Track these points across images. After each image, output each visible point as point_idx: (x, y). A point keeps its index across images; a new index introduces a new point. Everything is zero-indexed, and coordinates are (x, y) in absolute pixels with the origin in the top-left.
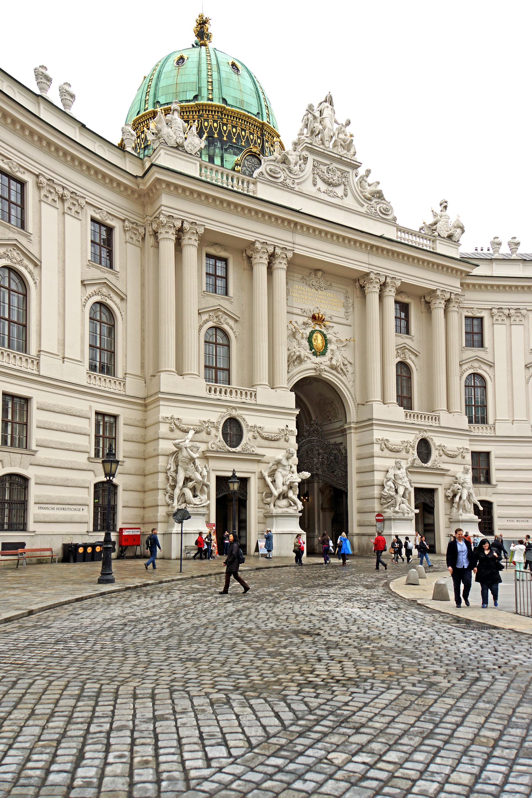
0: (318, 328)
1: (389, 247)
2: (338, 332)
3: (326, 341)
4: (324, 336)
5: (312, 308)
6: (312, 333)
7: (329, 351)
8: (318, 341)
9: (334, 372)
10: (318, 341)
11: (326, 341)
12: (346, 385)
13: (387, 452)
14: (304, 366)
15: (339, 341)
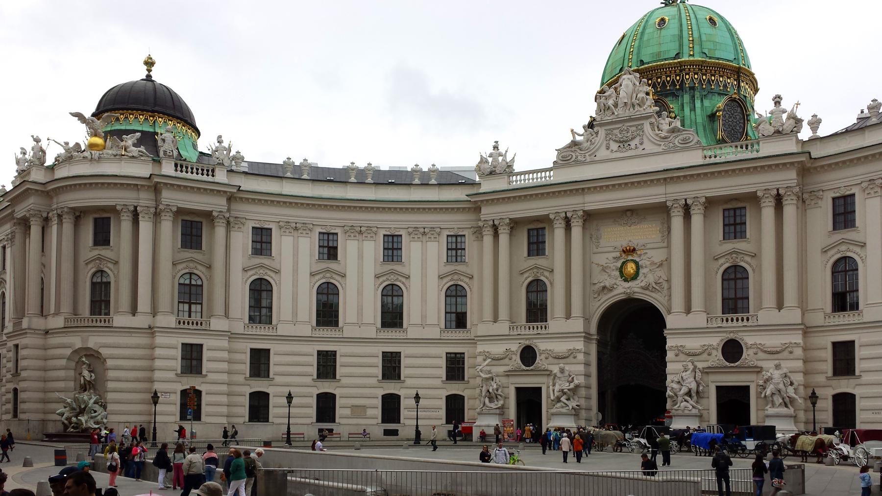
0: (630, 258)
1: (670, 175)
2: (652, 256)
3: (638, 267)
4: (636, 263)
5: (624, 243)
6: (624, 263)
7: (641, 275)
8: (631, 268)
9: (647, 292)
10: (631, 268)
11: (638, 267)
12: (656, 300)
13: (682, 357)
14: (615, 292)
15: (653, 263)
